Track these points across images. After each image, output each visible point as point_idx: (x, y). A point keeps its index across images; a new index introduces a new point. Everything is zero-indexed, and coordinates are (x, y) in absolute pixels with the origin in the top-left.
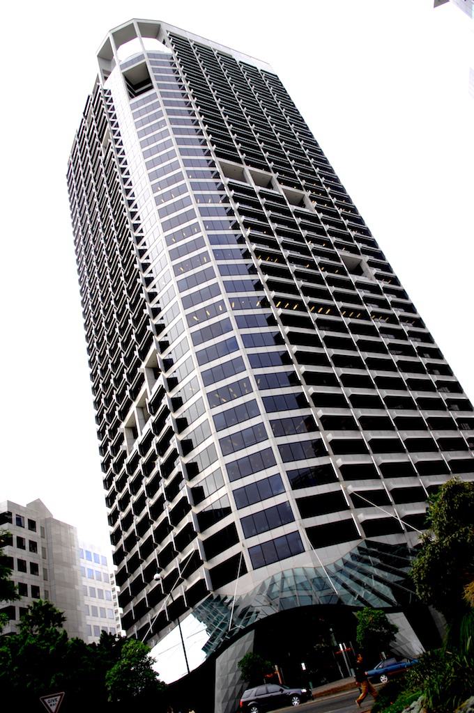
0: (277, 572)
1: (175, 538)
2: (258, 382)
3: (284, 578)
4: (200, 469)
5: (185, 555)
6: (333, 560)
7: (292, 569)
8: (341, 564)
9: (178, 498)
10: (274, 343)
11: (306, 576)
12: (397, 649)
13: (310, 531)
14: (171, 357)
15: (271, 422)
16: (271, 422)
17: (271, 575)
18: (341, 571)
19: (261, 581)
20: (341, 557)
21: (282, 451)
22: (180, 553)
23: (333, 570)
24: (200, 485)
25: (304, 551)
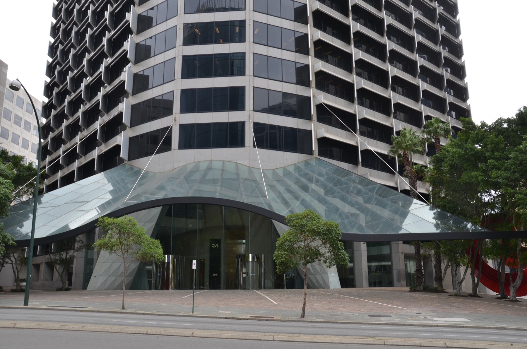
0: (208, 159)
1: (100, 157)
2: (256, 32)
3: (209, 169)
4: (154, 24)
5: (107, 147)
6: (273, 166)
7: (224, 161)
8: (280, 173)
9: (114, 113)
10: (292, 17)
11: (237, 174)
12: (317, 276)
13: (258, 128)
14: (151, 14)
15: (256, 124)
16: (256, 124)
17: (196, 161)
18: (279, 181)
19: (185, 163)
20: (283, 166)
21: (256, 63)
22: (103, 144)
23: (270, 175)
24: (146, 73)
25: (245, 10)
